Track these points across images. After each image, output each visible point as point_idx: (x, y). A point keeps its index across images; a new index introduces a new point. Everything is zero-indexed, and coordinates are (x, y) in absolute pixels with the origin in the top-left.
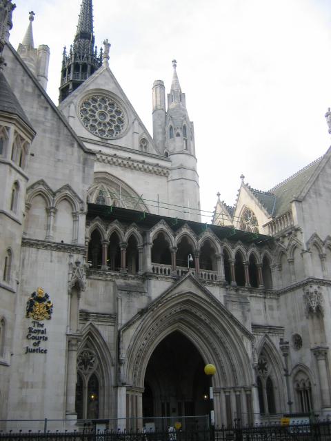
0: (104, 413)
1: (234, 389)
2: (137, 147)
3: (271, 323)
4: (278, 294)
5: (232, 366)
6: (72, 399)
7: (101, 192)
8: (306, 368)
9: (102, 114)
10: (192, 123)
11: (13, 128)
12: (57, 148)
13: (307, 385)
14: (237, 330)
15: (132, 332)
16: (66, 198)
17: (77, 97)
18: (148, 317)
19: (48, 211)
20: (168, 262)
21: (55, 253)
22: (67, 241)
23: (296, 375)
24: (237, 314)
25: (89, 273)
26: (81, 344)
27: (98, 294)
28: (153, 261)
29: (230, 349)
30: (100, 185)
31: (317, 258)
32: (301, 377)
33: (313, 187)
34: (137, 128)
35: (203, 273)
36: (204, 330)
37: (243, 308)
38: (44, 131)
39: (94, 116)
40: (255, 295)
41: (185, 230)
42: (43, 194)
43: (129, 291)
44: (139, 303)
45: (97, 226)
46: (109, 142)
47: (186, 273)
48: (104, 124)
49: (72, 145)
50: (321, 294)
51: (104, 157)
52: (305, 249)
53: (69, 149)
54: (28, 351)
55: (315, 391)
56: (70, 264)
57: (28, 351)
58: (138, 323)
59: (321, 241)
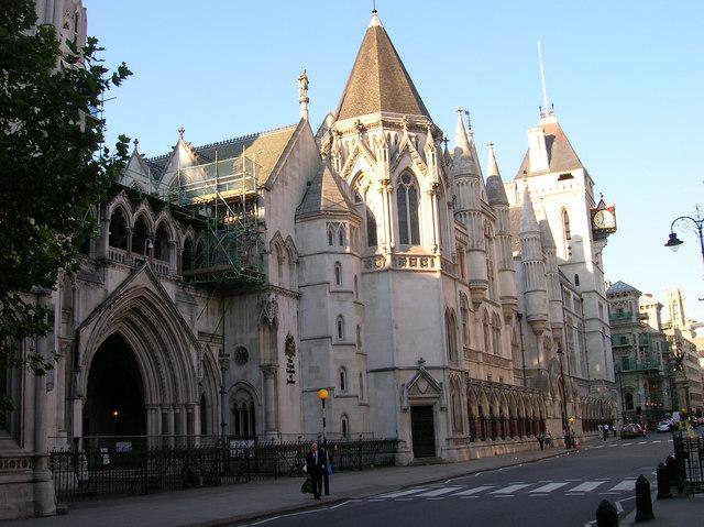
1: (174, 406)
5: (174, 377)
8: (252, 387)
10: (85, 9)
13: (248, 405)
20: (123, 247)
23: (234, 394)
24: (186, 318)
28: (112, 243)
29: (175, 360)
32: (241, 395)
36: (149, 335)
37: (191, 311)
41: (144, 207)
44: (97, 296)
47: (142, 262)
52: (268, 249)
55: (259, 413)
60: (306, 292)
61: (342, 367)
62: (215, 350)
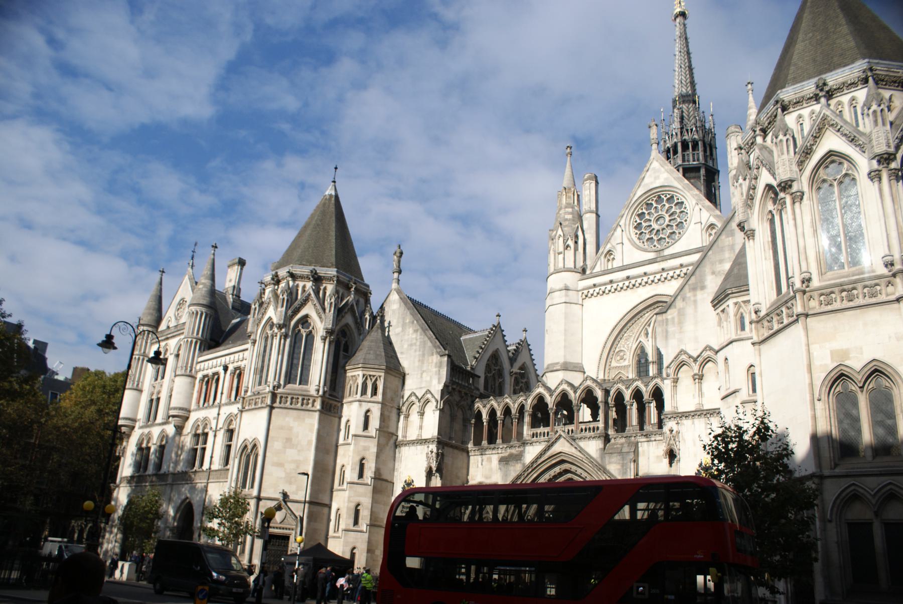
12: (422, 361)
16: (427, 401)
21: (419, 447)
33: (690, 282)
35: (584, 427)
38: (415, 351)
39: (650, 226)
40: (653, 439)
46: (667, 252)
48: (663, 229)
50: (678, 432)
51: (652, 278)
53: (430, 358)
56: (427, 454)
59: (690, 357)
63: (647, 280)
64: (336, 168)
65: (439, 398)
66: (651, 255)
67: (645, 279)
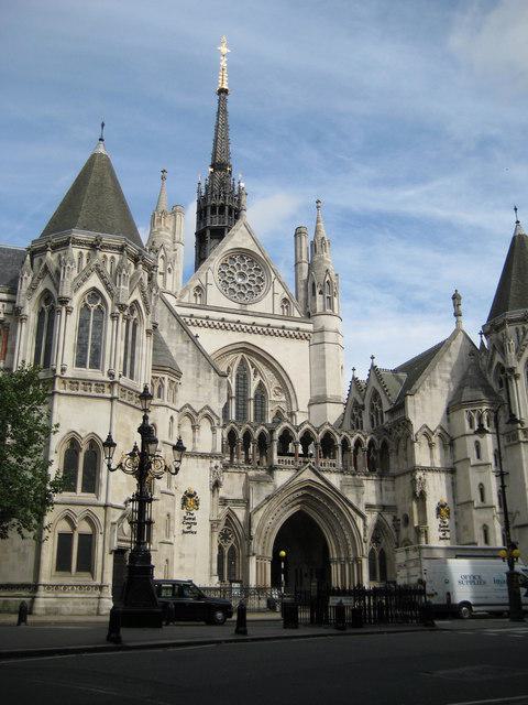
0: (239, 576)
2: (278, 311)
3: (386, 503)
4: (395, 477)
6: (215, 566)
7: (243, 361)
9: (242, 275)
11: (166, 377)
12: (198, 376)
14: (350, 510)
15: (260, 513)
16: (207, 416)
17: (215, 260)
18: (274, 503)
19: (193, 427)
21: (200, 460)
22: (208, 450)
25: (226, 467)
26: (222, 526)
27: (233, 485)
28: (279, 454)
30: (240, 355)
31: (425, 447)
34: (278, 288)
38: (188, 362)
42: (191, 415)
43: (258, 480)
44: (267, 490)
45: (232, 427)
46: (249, 308)
49: (210, 372)
51: (243, 326)
53: (207, 374)
54: (184, 532)
56: (211, 469)
57: (184, 532)
58: (265, 507)
60: (458, 466)
61: (485, 525)
62: (388, 518)
63: (237, 327)
64: (103, 125)
65: (221, 417)
66: (237, 306)
67: (238, 326)
